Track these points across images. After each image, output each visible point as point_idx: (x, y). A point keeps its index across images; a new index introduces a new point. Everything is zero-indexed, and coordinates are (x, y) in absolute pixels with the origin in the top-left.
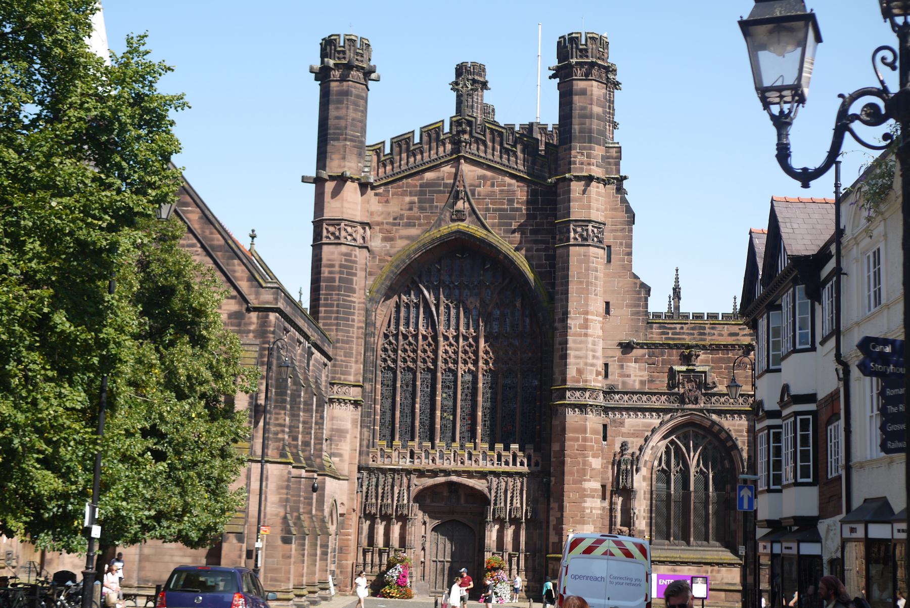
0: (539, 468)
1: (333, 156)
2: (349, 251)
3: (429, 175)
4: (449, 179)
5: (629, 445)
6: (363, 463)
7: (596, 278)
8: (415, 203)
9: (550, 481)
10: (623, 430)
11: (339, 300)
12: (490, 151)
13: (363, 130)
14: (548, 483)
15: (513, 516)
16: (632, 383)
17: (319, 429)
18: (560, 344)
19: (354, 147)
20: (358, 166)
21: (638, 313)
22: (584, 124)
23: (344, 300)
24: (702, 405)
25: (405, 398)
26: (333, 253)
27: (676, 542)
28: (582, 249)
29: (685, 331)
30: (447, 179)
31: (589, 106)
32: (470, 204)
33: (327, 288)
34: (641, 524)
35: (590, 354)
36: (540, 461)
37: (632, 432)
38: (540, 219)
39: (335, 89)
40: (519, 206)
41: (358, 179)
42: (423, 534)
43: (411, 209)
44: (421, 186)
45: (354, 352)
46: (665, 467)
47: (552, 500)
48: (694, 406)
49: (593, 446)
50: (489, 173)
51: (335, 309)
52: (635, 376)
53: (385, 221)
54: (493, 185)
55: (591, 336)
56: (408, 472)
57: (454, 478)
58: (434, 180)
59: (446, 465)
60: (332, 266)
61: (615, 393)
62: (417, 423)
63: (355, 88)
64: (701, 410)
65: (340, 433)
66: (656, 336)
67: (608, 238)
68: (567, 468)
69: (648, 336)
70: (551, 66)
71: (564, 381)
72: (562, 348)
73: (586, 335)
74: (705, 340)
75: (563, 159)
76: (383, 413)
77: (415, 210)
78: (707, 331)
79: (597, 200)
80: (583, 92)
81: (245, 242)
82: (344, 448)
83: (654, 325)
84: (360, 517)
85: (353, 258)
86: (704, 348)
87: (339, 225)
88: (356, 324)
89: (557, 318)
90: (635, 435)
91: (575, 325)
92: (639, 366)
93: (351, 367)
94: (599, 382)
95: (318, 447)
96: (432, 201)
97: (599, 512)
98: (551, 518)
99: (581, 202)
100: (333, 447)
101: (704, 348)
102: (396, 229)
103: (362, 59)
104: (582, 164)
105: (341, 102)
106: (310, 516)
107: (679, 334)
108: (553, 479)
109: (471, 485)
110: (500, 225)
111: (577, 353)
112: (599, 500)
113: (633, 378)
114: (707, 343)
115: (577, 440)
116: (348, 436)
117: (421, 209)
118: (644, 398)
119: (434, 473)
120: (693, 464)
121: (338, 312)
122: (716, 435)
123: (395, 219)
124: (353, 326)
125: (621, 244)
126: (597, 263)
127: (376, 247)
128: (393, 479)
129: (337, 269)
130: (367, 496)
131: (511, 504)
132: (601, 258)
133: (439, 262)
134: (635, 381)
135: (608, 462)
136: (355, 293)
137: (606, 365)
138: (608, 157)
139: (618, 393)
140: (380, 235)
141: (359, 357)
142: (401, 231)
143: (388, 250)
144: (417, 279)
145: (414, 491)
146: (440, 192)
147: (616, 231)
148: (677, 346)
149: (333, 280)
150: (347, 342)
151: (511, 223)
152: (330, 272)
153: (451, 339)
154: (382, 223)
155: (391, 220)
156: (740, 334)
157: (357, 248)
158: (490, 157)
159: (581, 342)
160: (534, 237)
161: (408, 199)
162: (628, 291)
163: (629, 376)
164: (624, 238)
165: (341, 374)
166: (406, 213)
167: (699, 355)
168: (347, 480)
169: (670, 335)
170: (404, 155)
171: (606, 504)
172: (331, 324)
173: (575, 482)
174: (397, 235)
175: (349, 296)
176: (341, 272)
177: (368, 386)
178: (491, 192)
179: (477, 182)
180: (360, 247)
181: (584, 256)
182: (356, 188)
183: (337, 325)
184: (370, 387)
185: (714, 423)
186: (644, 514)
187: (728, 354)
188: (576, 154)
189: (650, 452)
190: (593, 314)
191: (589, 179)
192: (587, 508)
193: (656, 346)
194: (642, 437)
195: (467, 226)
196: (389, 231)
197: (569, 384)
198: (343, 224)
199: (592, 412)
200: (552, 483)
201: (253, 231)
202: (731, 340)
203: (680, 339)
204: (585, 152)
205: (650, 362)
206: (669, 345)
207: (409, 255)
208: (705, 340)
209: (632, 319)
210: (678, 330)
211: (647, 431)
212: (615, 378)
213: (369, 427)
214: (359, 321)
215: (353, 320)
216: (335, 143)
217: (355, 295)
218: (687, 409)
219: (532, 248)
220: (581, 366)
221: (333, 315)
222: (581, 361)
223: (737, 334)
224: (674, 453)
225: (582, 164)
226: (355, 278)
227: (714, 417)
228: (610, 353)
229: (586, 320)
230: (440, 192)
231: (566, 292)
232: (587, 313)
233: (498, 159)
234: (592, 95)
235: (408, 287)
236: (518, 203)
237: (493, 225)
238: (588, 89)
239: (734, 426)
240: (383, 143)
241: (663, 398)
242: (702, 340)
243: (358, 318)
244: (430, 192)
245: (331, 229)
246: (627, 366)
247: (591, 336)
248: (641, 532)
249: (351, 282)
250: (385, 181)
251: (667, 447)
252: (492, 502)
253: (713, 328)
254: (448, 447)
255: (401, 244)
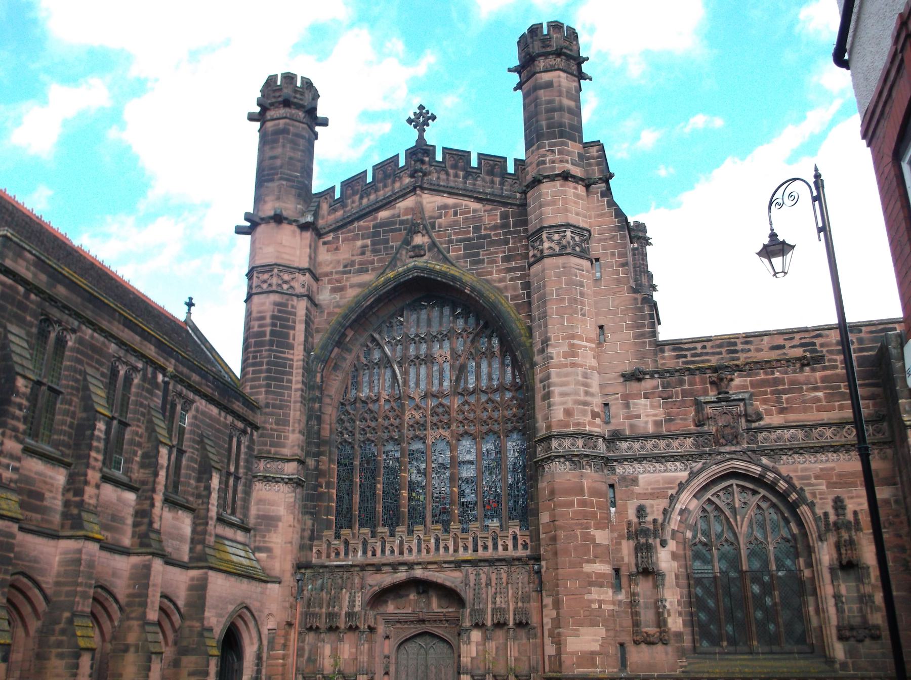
0: (528, 552)
1: (267, 199)
2: (284, 301)
3: (383, 214)
4: (407, 215)
5: (648, 510)
6: (303, 560)
7: (582, 294)
8: (367, 246)
9: (540, 566)
10: (638, 490)
11: (270, 356)
12: (452, 178)
13: (308, 172)
14: (539, 572)
15: (496, 621)
16: (642, 425)
17: (203, 503)
18: (541, 381)
19: (292, 187)
20: (296, 208)
21: (642, 335)
22: (553, 118)
23: (276, 357)
24: (745, 446)
25: (366, 479)
26: (263, 304)
27: (732, 649)
28: (560, 260)
29: (708, 350)
30: (403, 216)
31: (557, 99)
32: (430, 237)
33: (257, 344)
34: (675, 623)
35: (582, 388)
36: (528, 541)
37: (650, 491)
38: (513, 243)
39: (271, 129)
40: (487, 232)
41: (296, 221)
42: (386, 652)
43: (363, 253)
44: (374, 227)
45: (291, 421)
46: (704, 539)
47: (544, 593)
48: (733, 449)
49: (595, 513)
50: (450, 201)
51: (265, 367)
52: (647, 416)
53: (334, 271)
54: (455, 214)
55: (581, 366)
56: (363, 567)
57: (418, 573)
58: (389, 218)
59: (406, 557)
60: (263, 318)
61: (620, 440)
62: (380, 509)
63: (293, 126)
64: (745, 452)
65: (270, 521)
66: (668, 360)
67: (596, 248)
68: (560, 545)
69: (660, 362)
70: (512, 66)
71: (549, 427)
72: (544, 386)
73: (573, 365)
74: (738, 359)
75: (531, 163)
76: (340, 499)
77: (368, 253)
78: (740, 347)
79: (575, 203)
80: (549, 85)
81: (180, 314)
82: (274, 540)
83: (667, 347)
84: (300, 633)
85: (290, 309)
86: (738, 368)
87: (272, 271)
88: (294, 386)
89: (535, 350)
90: (654, 495)
91: (558, 354)
92: (651, 402)
93: (286, 438)
94: (599, 426)
95: (200, 528)
96: (387, 241)
97: (611, 607)
98: (545, 620)
99: (555, 205)
100: (258, 538)
101: (738, 368)
102: (347, 278)
103: (301, 97)
104: (553, 162)
105: (276, 141)
106: (140, 622)
107: (701, 355)
108: (543, 563)
109: (439, 581)
110: (466, 256)
111: (563, 389)
112: (610, 591)
113: (643, 419)
114: (741, 362)
115: (571, 504)
116: (280, 524)
117: (375, 251)
118: (662, 443)
119: (395, 566)
120: (743, 529)
121: (269, 371)
122: (771, 487)
123: (345, 266)
124: (290, 388)
125: (613, 254)
126: (582, 276)
127: (324, 300)
128: (342, 578)
129: (268, 321)
130: (309, 606)
131: (494, 603)
132: (587, 271)
133: (402, 316)
134: (646, 422)
135: (621, 537)
136: (293, 349)
137: (606, 405)
138: (588, 158)
139: (625, 439)
140: (329, 286)
141: (297, 425)
142: (352, 279)
143: (337, 302)
144: (377, 336)
145: (369, 592)
146: (395, 230)
147: (605, 240)
148: (702, 371)
149: (262, 334)
150: (281, 407)
151: (479, 252)
152: (260, 326)
153: (417, 400)
154: (331, 273)
155: (341, 269)
156: (787, 346)
157: (295, 298)
158: (452, 184)
159: (567, 375)
160: (506, 265)
161: (359, 243)
162: (627, 310)
163: (638, 417)
164: (616, 246)
165: (270, 446)
166: (358, 259)
167: (732, 380)
168: (280, 583)
169: (689, 359)
170: (357, 198)
171: (622, 596)
172: (260, 386)
173: (573, 565)
174: (348, 284)
175: (284, 353)
176: (274, 325)
177: (311, 462)
178: (454, 221)
179: (437, 213)
180: (298, 296)
181: (564, 267)
182: (294, 232)
183: (269, 386)
184: (313, 462)
185: (765, 468)
186: (680, 609)
187: (773, 373)
188: (545, 152)
189: (679, 518)
190: (581, 338)
191: (566, 176)
192: (591, 601)
193: (672, 372)
194: (664, 497)
195: (427, 261)
196: (338, 281)
197: (555, 430)
198: (276, 270)
199: (590, 466)
200: (543, 570)
201: (191, 299)
202: (774, 355)
203: (703, 362)
204: (556, 149)
205: (664, 395)
206: (688, 370)
207: (358, 303)
208: (738, 359)
209: (635, 344)
210: (699, 351)
211: (671, 488)
212: (620, 421)
213: (311, 514)
214: (297, 382)
215: (290, 381)
216: (270, 184)
217: (291, 352)
218: (723, 453)
219: (505, 278)
220: (570, 405)
221: (263, 375)
222: (570, 399)
223: (782, 347)
224: (711, 511)
225: (553, 162)
226: (292, 332)
227: (765, 461)
228: (610, 390)
229: (572, 346)
230: (395, 230)
231: (544, 316)
232: (573, 337)
233: (461, 186)
234: (559, 86)
235: (367, 346)
236: (486, 229)
237: (458, 258)
238: (555, 80)
239: (796, 471)
240: (333, 188)
241: (689, 441)
242: (733, 359)
243: (297, 379)
244: (384, 232)
245: (266, 276)
246: (634, 404)
247: (581, 366)
248: (679, 635)
249: (287, 336)
250: (334, 226)
251: (704, 510)
252: (468, 605)
253: (747, 343)
254: (411, 532)
255: (351, 294)
